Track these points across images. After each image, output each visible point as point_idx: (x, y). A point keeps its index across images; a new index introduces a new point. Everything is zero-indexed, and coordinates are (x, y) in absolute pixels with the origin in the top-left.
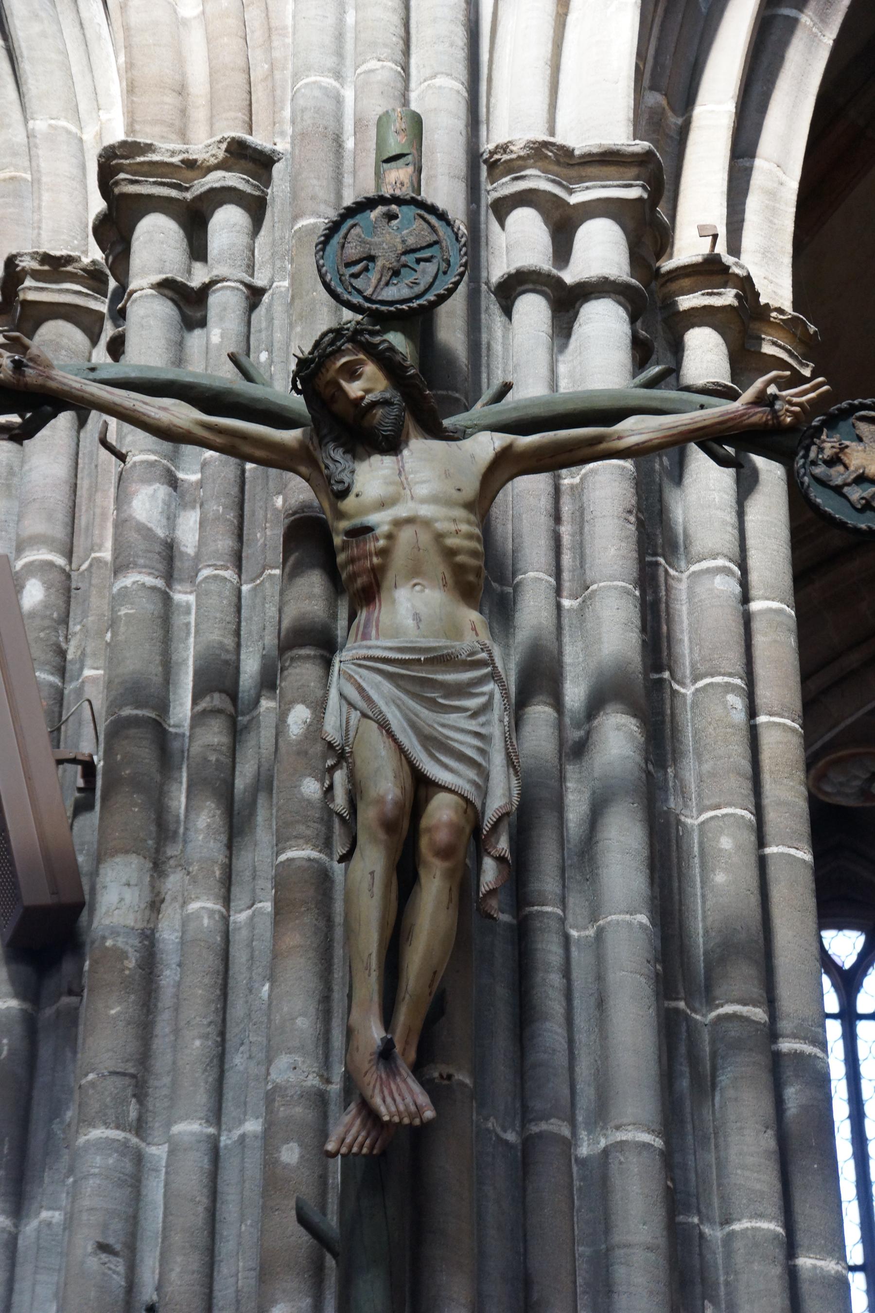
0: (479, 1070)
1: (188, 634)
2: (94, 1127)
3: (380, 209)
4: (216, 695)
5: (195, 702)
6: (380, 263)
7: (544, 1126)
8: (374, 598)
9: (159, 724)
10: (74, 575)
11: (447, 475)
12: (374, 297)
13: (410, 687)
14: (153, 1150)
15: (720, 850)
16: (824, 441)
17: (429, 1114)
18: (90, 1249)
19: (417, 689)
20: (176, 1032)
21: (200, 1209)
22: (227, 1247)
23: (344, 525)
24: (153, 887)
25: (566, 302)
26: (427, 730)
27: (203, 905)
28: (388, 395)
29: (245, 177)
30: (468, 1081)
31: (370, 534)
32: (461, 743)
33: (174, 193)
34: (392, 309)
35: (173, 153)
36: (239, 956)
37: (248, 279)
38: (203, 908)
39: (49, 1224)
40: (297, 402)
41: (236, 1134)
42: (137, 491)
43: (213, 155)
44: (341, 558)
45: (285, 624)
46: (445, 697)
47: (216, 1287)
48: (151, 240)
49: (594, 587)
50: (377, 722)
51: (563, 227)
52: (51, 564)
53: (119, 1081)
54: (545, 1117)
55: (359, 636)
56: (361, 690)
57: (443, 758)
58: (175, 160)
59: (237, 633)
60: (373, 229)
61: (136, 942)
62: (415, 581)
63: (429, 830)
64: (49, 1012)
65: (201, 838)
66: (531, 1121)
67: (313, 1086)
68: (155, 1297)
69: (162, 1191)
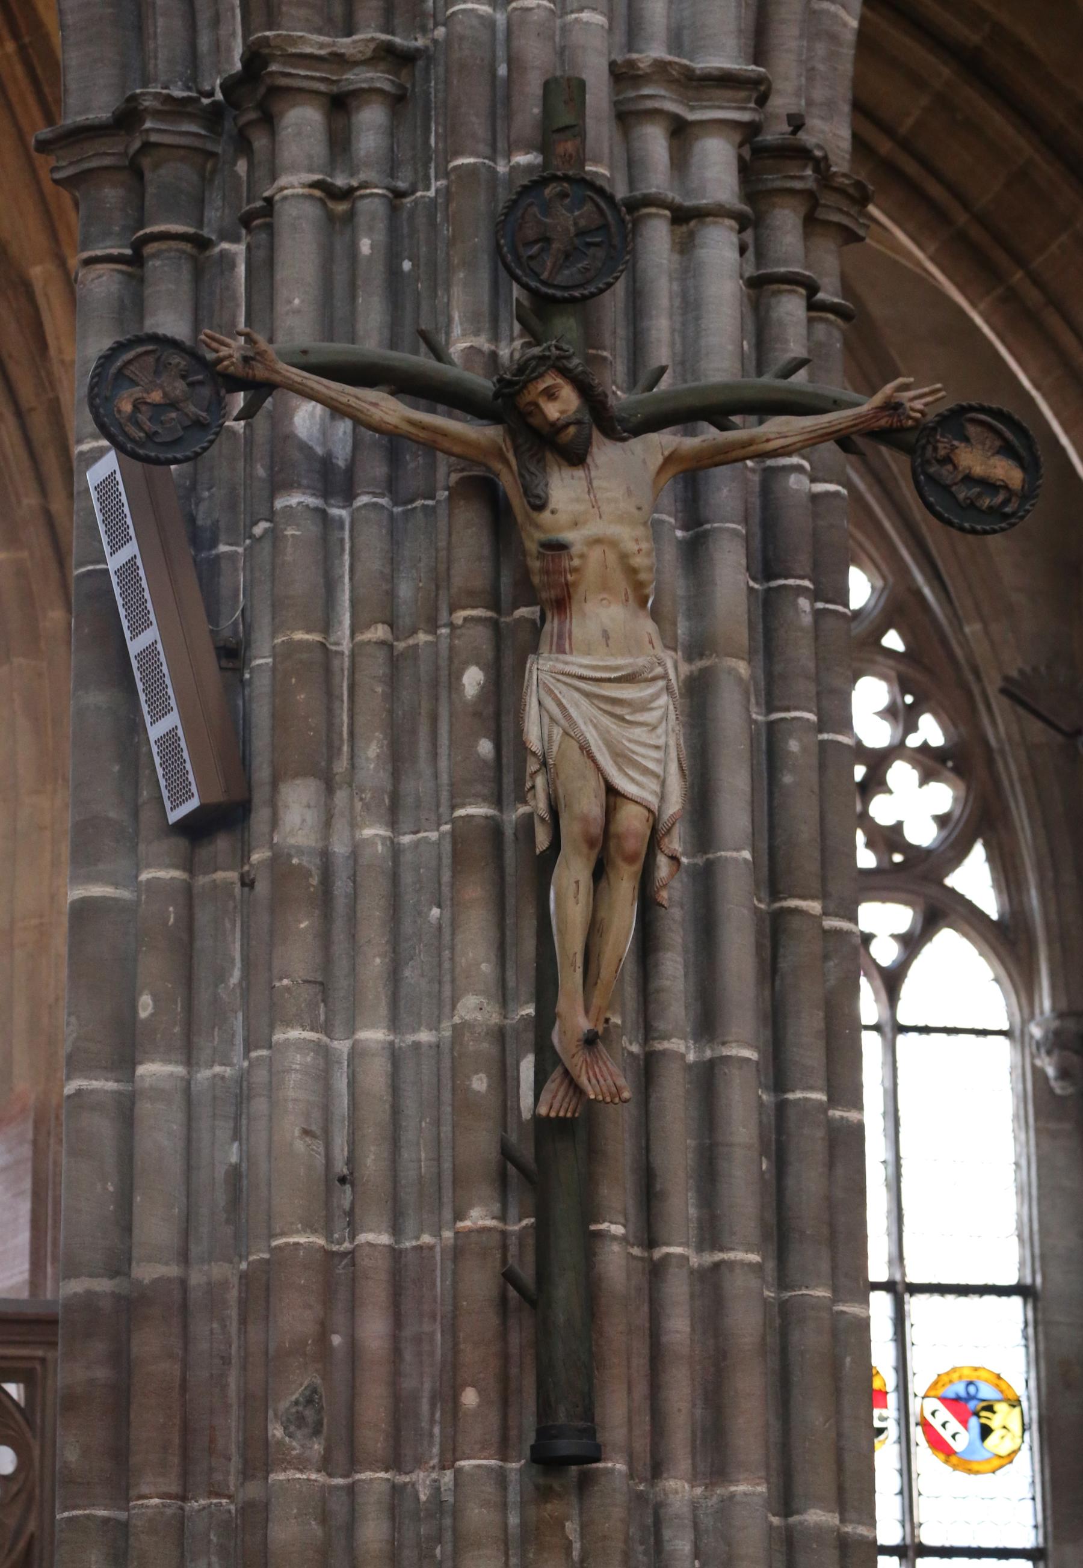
1: (343, 550)
2: (292, 1028)
4: (380, 626)
6: (555, 246)
7: (666, 1045)
8: (565, 609)
9: (323, 645)
13: (602, 706)
14: (336, 1044)
15: (789, 752)
16: (938, 441)
18: (297, 1133)
19: (608, 707)
21: (387, 1106)
22: (409, 1135)
23: (539, 536)
24: (326, 805)
28: (579, 416)
29: (390, 77)
31: (565, 552)
32: (643, 756)
34: (566, 295)
35: (322, 46)
36: (407, 878)
38: (377, 835)
39: (223, 1078)
42: (298, 407)
43: (360, 52)
46: (631, 714)
48: (299, 134)
49: (708, 526)
50: (578, 742)
55: (554, 647)
57: (630, 773)
61: (318, 861)
62: (605, 596)
65: (372, 766)
66: (654, 1039)
67: (496, 1024)
68: (345, 1171)
69: (345, 1081)
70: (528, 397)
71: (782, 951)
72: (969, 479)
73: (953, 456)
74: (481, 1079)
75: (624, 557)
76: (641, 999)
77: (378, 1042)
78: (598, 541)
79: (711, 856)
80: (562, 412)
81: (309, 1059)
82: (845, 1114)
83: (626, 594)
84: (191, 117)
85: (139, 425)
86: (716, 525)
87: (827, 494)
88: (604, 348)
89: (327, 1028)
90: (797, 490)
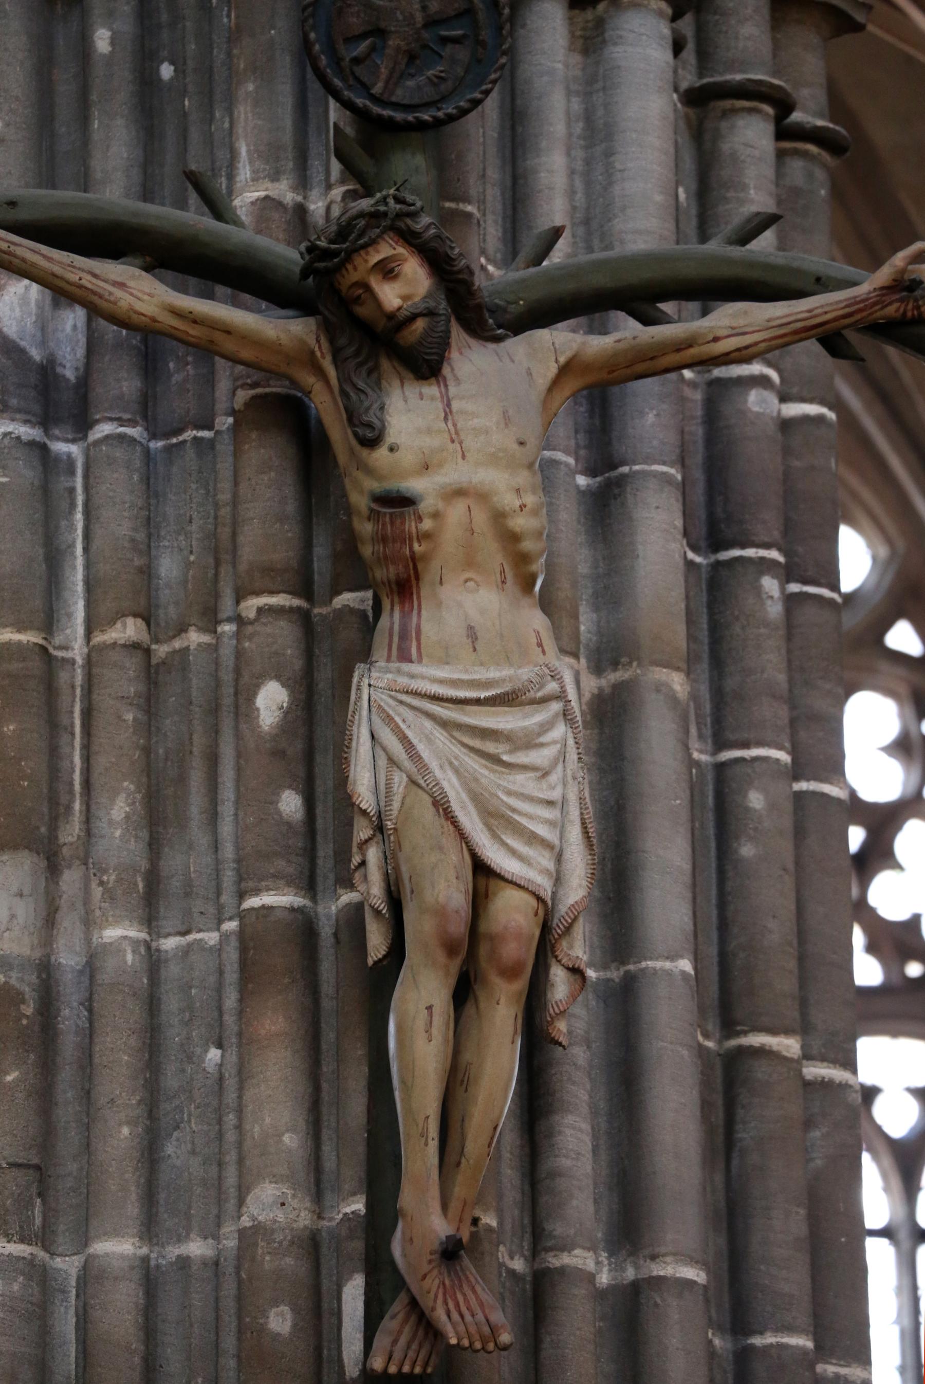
1: (73, 505)
4: (130, 621)
9: (44, 649)
14: (58, 1262)
15: (748, 810)
19: (477, 743)
21: (137, 1360)
28: (432, 304)
31: (411, 509)
32: (531, 817)
36: (171, 1003)
38: (125, 937)
46: (511, 752)
49: (625, 469)
54: (565, 1247)
57: (509, 841)
61: (34, 978)
62: (467, 575)
65: (118, 833)
66: (551, 1249)
67: (306, 1227)
70: (352, 275)
71: (740, 1113)
74: (282, 1314)
75: (499, 517)
76: (527, 1187)
77: (123, 1257)
78: (460, 492)
79: (631, 967)
80: (405, 298)
81: (16, 1287)
82: (843, 1371)
83: (503, 572)
86: (637, 468)
87: (806, 419)
88: (466, 200)
89: (44, 1238)
90: (758, 415)
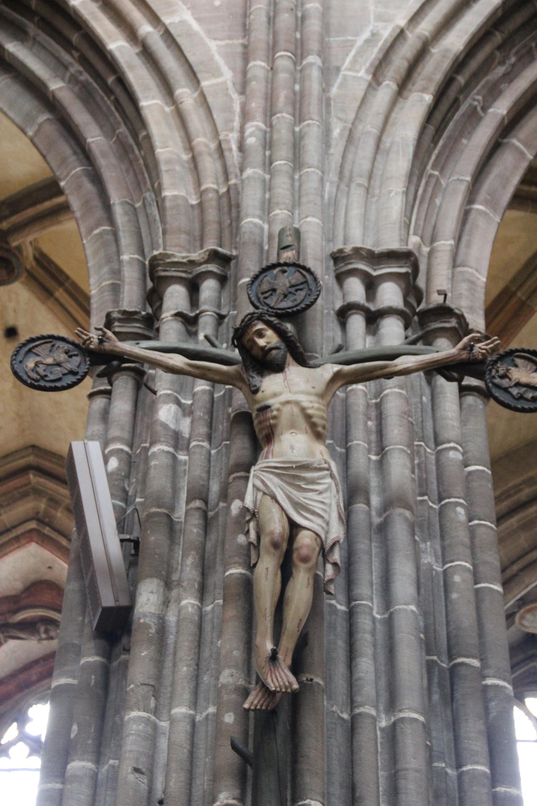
0: (328, 679)
2: (133, 711)
3: (278, 269)
5: (188, 503)
7: (362, 710)
9: (168, 516)
10: (133, 456)
11: (308, 381)
12: (275, 307)
13: (287, 480)
15: (454, 582)
17: (296, 686)
18: (130, 771)
19: (291, 481)
20: (175, 665)
21: (185, 751)
22: (199, 770)
23: (257, 406)
24: (164, 595)
25: (373, 319)
26: (296, 500)
27: (189, 602)
28: (278, 345)
30: (321, 682)
33: (184, 275)
36: (207, 627)
37: (218, 311)
40: (236, 354)
41: (204, 714)
42: (161, 408)
44: (256, 422)
45: (231, 462)
47: (194, 790)
48: (172, 296)
49: (387, 449)
51: (371, 285)
52: (122, 450)
53: (146, 688)
54: (362, 705)
56: (263, 482)
58: (185, 260)
59: (209, 472)
60: (275, 277)
61: (156, 621)
62: (292, 431)
63: (297, 549)
64: (115, 664)
66: (356, 707)
67: (242, 685)
68: (163, 796)
70: (248, 337)
71: (455, 687)
72: (518, 384)
73: (508, 374)
74: (230, 716)
75: (303, 410)
76: (349, 689)
77: (181, 713)
78: (288, 402)
79: (392, 610)
80: (268, 343)
81: (141, 727)
82: (508, 790)
83: (306, 429)
84: (137, 321)
85: (37, 373)
86: (391, 447)
87: (478, 471)
88: (316, 353)
89: (156, 712)
90: (453, 458)
